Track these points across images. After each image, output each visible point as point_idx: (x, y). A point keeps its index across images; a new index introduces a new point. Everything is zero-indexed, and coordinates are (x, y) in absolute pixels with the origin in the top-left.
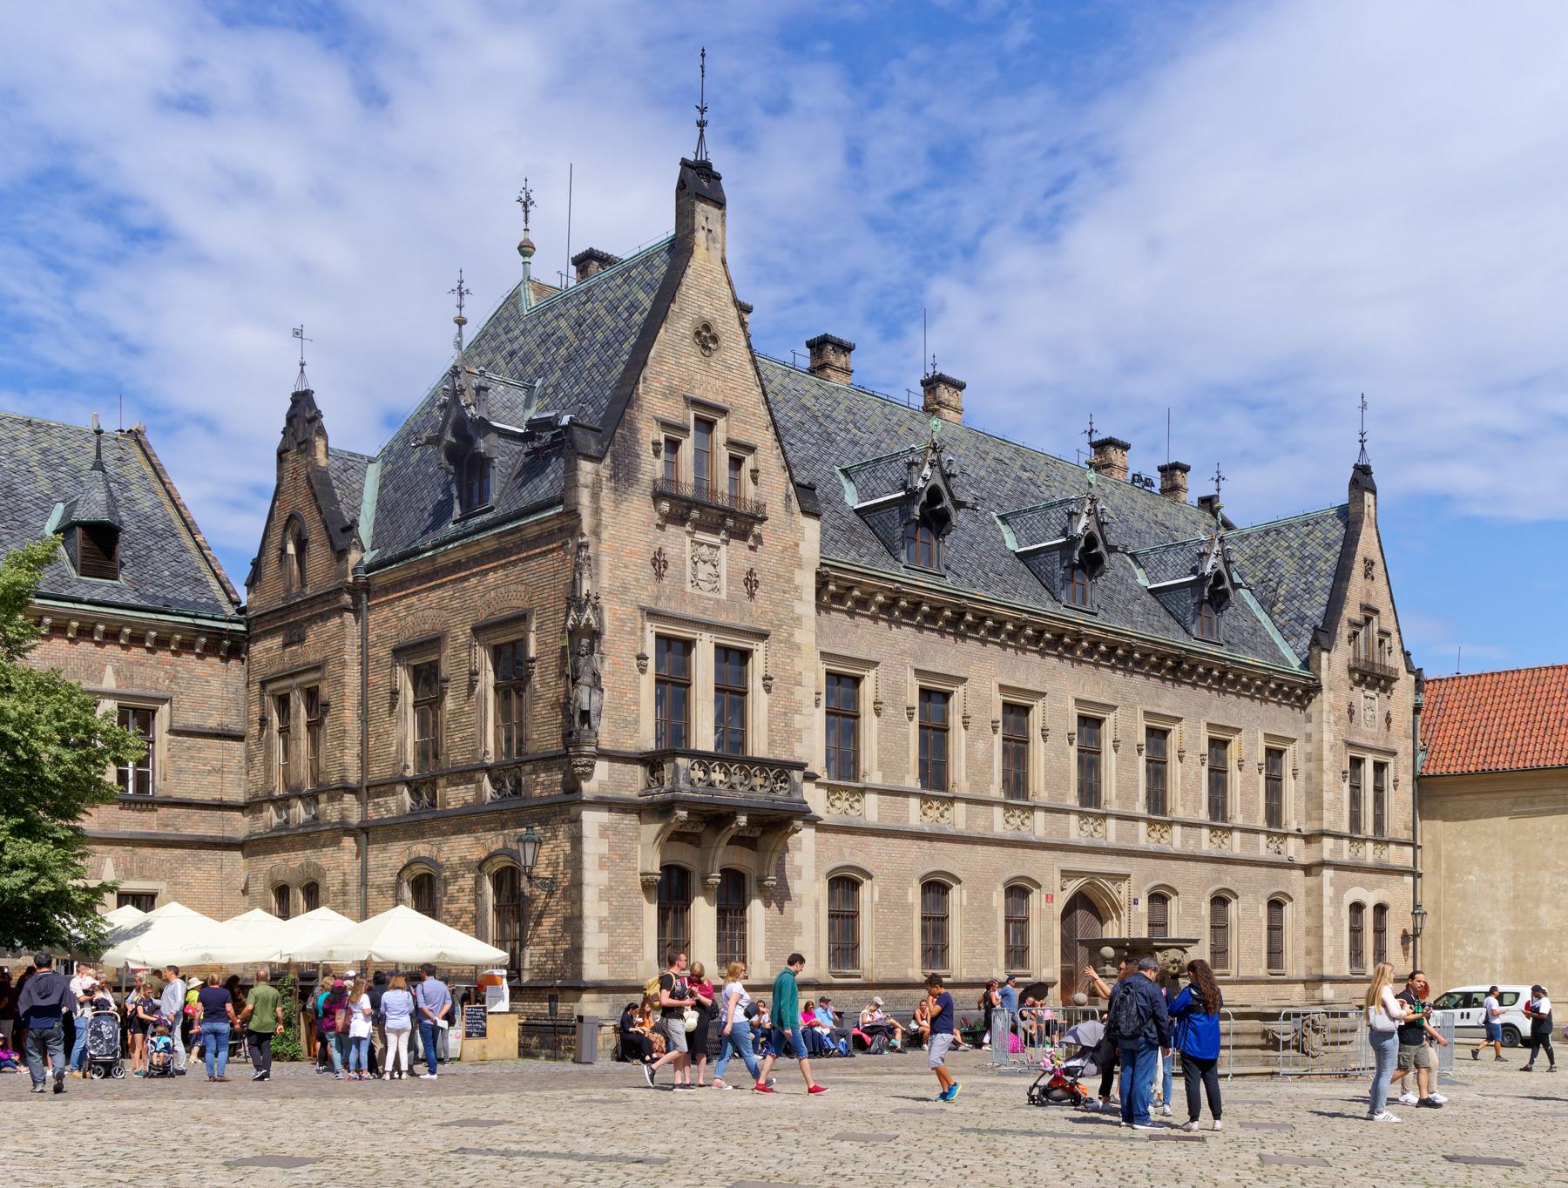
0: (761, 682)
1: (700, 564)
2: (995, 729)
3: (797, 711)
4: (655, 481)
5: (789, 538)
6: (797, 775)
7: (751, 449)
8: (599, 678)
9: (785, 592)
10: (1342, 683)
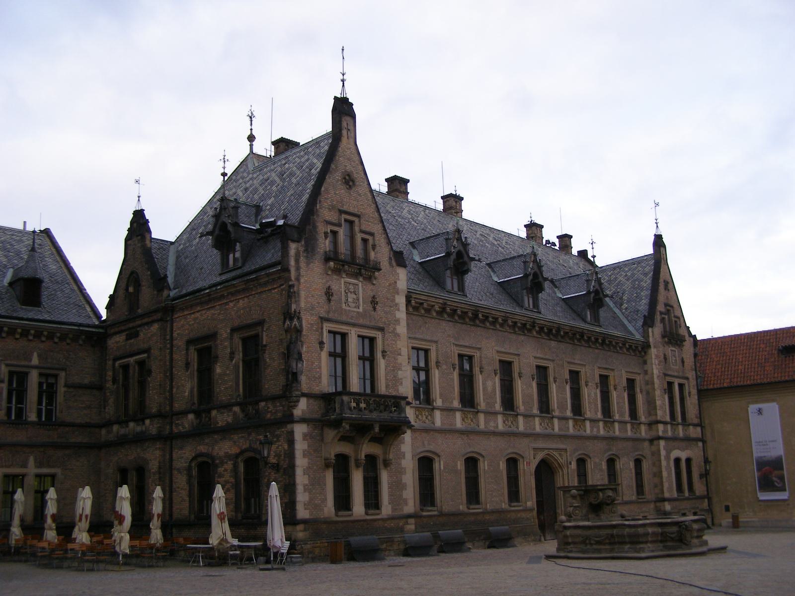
0: (381, 353)
1: (349, 294)
2: (496, 374)
3: (400, 369)
4: (326, 252)
6: (403, 403)
7: (372, 234)
8: (301, 355)
9: (391, 307)
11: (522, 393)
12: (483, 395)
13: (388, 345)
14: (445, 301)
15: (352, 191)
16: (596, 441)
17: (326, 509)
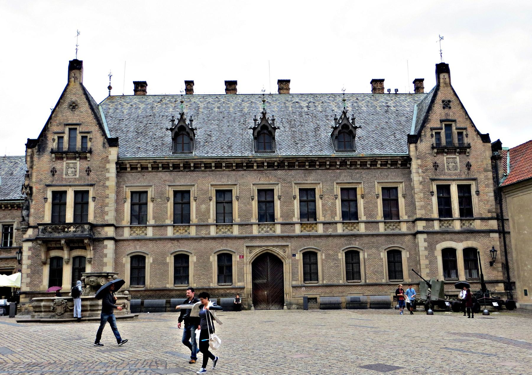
3: (107, 205)
5: (104, 155)
9: (102, 171)
10: (427, 155)
11: (239, 209)
12: (196, 214)
13: (98, 193)
14: (154, 161)
15: (76, 111)
16: (330, 239)
17: (42, 287)
